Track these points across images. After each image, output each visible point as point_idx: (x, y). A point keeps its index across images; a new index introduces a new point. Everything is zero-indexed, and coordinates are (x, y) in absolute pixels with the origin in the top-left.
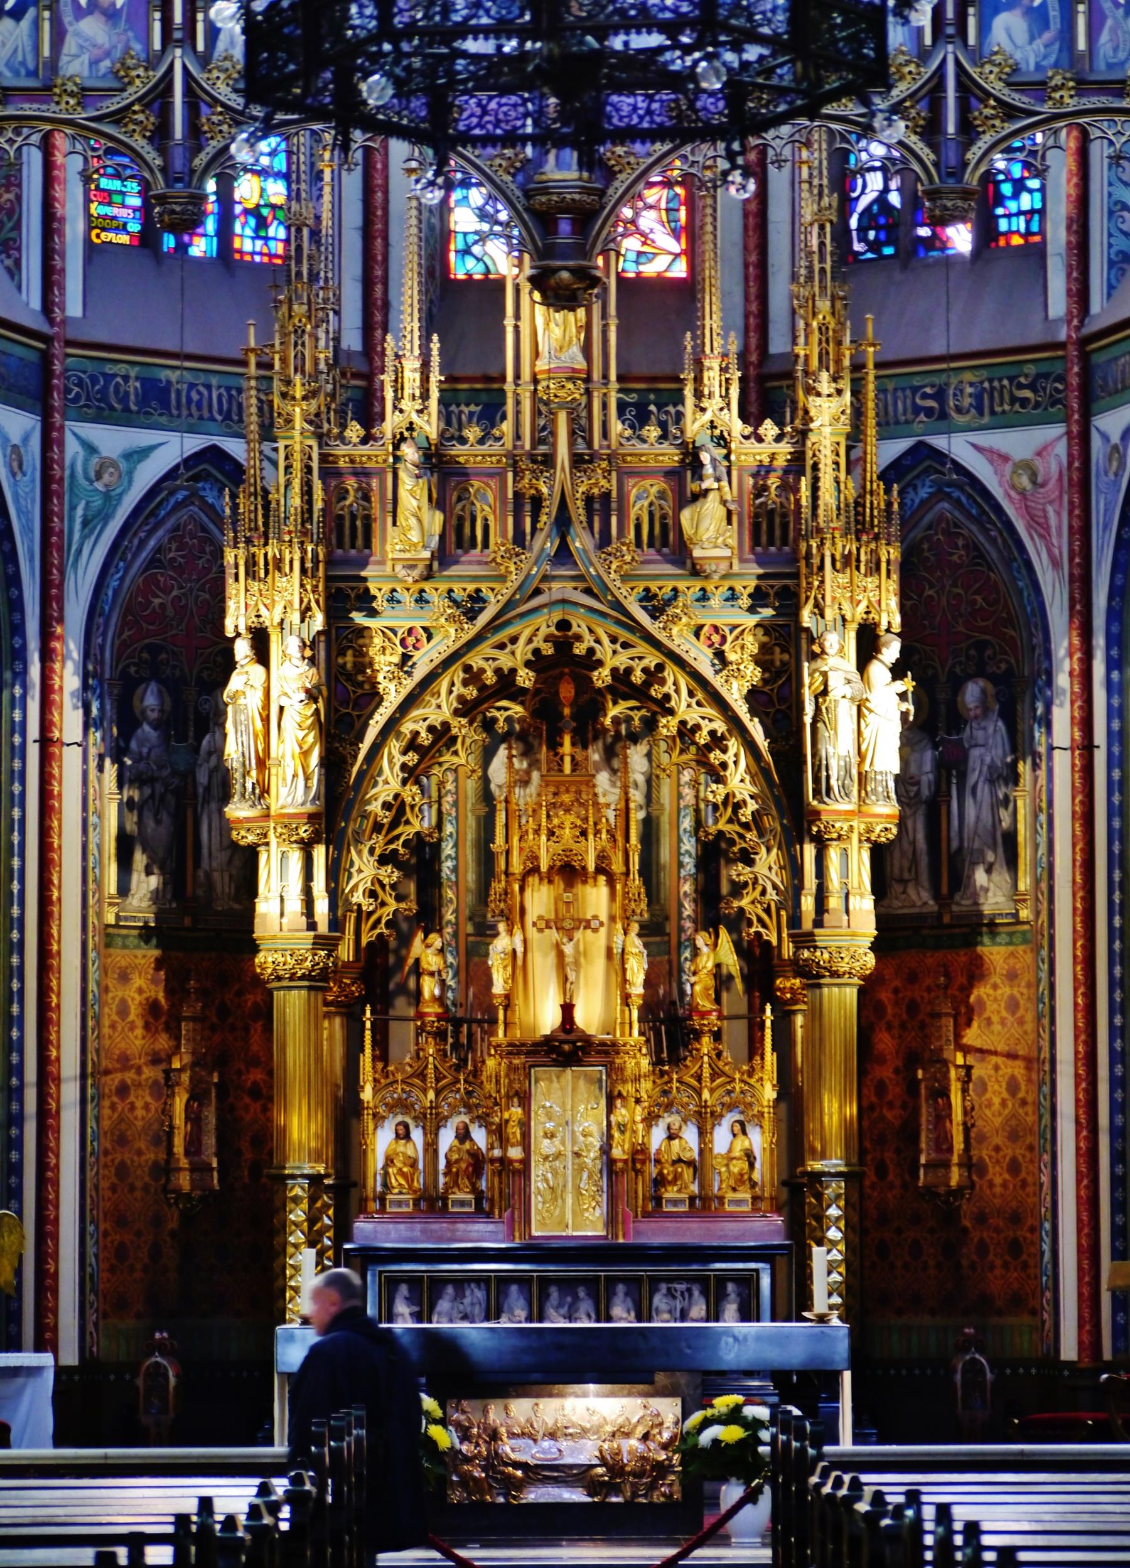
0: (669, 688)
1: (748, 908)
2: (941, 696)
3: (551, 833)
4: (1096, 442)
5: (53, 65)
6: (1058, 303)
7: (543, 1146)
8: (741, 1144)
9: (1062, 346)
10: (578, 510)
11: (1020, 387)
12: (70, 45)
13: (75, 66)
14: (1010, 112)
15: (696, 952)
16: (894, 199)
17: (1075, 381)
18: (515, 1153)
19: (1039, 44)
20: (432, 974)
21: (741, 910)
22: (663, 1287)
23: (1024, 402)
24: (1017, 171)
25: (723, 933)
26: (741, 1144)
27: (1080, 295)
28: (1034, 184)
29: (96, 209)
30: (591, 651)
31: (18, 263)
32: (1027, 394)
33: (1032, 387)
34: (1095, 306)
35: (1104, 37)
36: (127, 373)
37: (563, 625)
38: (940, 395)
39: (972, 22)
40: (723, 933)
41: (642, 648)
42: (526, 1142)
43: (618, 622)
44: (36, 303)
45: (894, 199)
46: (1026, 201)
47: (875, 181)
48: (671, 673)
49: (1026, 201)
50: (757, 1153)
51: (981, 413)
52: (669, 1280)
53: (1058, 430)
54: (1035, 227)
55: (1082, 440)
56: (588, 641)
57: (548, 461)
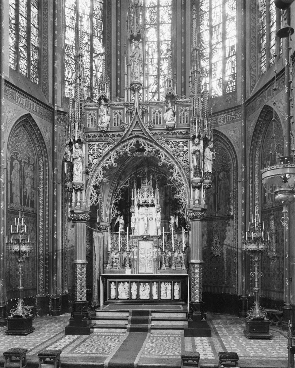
0: (160, 155)
1: (181, 212)
2: (217, 175)
3: (142, 196)
7: (141, 256)
8: (180, 255)
9: (241, 105)
11: (232, 115)
15: (170, 219)
18: (135, 257)
20: (122, 224)
21: (180, 212)
22: (163, 283)
23: (233, 118)
24: (231, 79)
25: (177, 216)
26: (180, 255)
28: (234, 81)
30: (144, 147)
31: (47, 94)
32: (234, 117)
33: (234, 115)
37: (138, 142)
40: (177, 216)
41: (155, 146)
42: (138, 254)
43: (150, 141)
44: (51, 101)
46: (233, 84)
48: (161, 151)
49: (233, 84)
50: (182, 256)
51: (224, 122)
52: (164, 282)
54: (234, 88)
56: (143, 145)
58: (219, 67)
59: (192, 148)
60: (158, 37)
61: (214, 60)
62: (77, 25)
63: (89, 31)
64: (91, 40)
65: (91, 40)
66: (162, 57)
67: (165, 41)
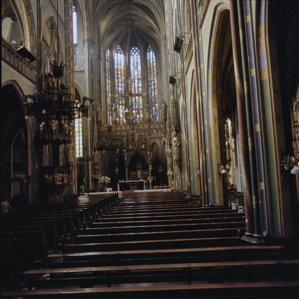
6: (160, 136)
27: (161, 135)
59: (148, 153)
63: (122, 117)
64: (123, 119)
65: (123, 119)
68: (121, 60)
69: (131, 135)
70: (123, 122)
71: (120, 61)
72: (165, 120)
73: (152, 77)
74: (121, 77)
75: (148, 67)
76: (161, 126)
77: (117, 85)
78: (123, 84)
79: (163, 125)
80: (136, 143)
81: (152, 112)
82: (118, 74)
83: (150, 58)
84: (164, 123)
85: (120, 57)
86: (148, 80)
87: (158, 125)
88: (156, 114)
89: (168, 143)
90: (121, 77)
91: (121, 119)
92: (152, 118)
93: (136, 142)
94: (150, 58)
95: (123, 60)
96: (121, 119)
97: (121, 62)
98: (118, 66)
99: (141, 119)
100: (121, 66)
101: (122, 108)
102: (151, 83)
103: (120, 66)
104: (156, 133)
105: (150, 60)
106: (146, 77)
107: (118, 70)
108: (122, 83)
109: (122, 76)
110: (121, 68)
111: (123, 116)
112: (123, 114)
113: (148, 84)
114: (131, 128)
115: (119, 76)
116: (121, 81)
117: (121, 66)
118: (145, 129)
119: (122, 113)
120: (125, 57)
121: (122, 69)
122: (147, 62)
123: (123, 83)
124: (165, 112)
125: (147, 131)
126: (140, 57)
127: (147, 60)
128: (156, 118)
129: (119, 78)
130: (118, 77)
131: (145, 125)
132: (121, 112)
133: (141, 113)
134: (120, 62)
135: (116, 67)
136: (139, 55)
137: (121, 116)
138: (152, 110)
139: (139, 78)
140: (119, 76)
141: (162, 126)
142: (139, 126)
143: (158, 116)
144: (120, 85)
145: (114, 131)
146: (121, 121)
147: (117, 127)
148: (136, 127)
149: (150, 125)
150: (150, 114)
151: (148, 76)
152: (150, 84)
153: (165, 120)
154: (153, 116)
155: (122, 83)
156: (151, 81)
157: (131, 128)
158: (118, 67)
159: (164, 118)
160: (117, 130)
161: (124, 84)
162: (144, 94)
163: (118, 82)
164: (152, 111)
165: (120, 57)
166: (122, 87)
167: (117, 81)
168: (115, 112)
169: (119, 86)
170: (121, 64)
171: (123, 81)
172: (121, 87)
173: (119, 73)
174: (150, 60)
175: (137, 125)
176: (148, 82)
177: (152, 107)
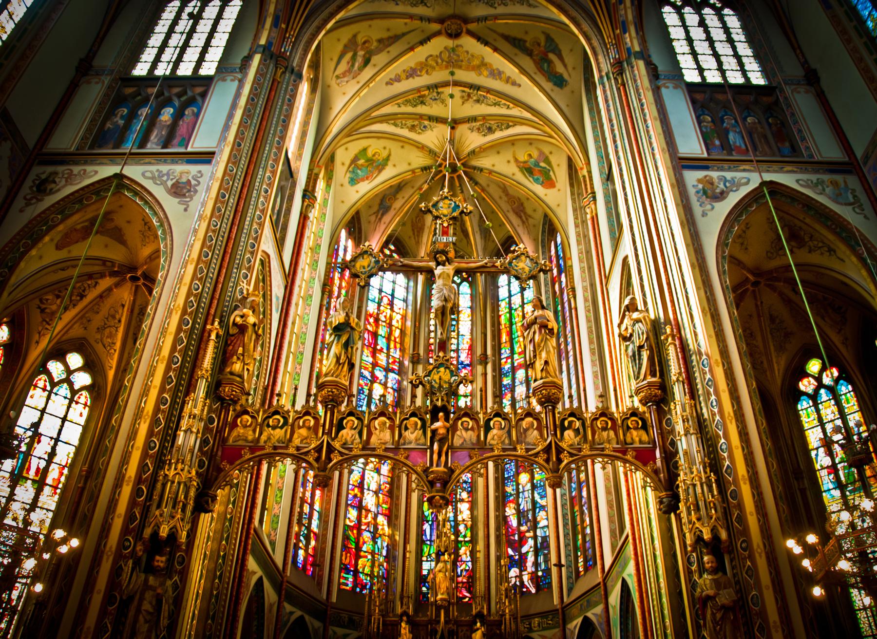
4: (567, 631)
5: (290, 440)
6: (556, 601)
9: (557, 610)
10: (446, 634)
12: (296, 436)
13: (296, 441)
14: (571, 455)
16: (518, 583)
17: (560, 617)
19: (578, 438)
29: (342, 581)
34: (565, 600)
35: (596, 437)
36: (345, 616)
38: (530, 624)
39: (558, 433)
45: (518, 583)
47: (513, 580)
53: (557, 630)
55: (564, 631)
57: (439, 622)
58: (531, 558)
60: (456, 516)
61: (524, 550)
62: (361, 501)
63: (373, 509)
64: (375, 518)
65: (375, 518)
66: (460, 539)
67: (464, 520)
68: (393, 290)
69: (432, 484)
70: (376, 528)
71: (390, 292)
72: (659, 398)
73: (516, 356)
74: (388, 348)
75: (499, 324)
76: (635, 433)
77: (367, 374)
78: (391, 376)
79: (645, 427)
80: (438, 615)
81: (518, 493)
82: (375, 335)
83: (510, 291)
84: (652, 418)
85: (394, 282)
86: (501, 369)
87: (614, 428)
88: (534, 503)
89: (707, 536)
90: (388, 348)
91: (370, 518)
92: (514, 522)
93: (438, 608)
94: (510, 291)
95: (400, 293)
96: (370, 518)
97: (393, 296)
98: (382, 308)
99: (461, 528)
100: (392, 309)
101: (378, 470)
102: (514, 379)
103: (389, 312)
104: (533, 591)
105: (510, 296)
106: (494, 355)
107: (377, 320)
108: (387, 370)
109: (392, 345)
110: (391, 318)
111: (378, 505)
112: (378, 496)
113: (501, 381)
114: (434, 432)
115: (379, 342)
116: (388, 363)
117: (392, 309)
118: (528, 450)
119: (376, 493)
120: (412, 284)
121: (394, 323)
122: (499, 306)
123: (392, 371)
124: (651, 349)
125: (540, 460)
126: (469, 291)
127: (496, 299)
128: (535, 523)
129: (381, 350)
130: (376, 344)
131: (525, 424)
132: (374, 487)
133: (462, 500)
134: (390, 297)
135: (372, 308)
136: (465, 283)
137: (370, 500)
138: (518, 484)
139: (462, 363)
140: (382, 343)
141: (637, 437)
142: (488, 429)
143: (543, 508)
144: (380, 374)
145: (319, 449)
146: (368, 524)
147: (340, 427)
148: (464, 436)
149: (563, 429)
150: (505, 506)
151: (500, 354)
152: (506, 381)
153: (659, 398)
154: (520, 513)
155: (387, 370)
156: (514, 369)
157: (434, 432)
158: (378, 308)
159: (650, 385)
160: (337, 445)
161: (397, 377)
162: (521, 265)
163: (375, 365)
164: (518, 489)
165: (394, 282)
166: (389, 385)
167: (370, 359)
168: (344, 339)
169: (374, 379)
170: (391, 304)
171: (394, 362)
172: (385, 385)
173: (382, 331)
174: (510, 296)
175: (477, 421)
176: (499, 373)
177: (518, 473)
